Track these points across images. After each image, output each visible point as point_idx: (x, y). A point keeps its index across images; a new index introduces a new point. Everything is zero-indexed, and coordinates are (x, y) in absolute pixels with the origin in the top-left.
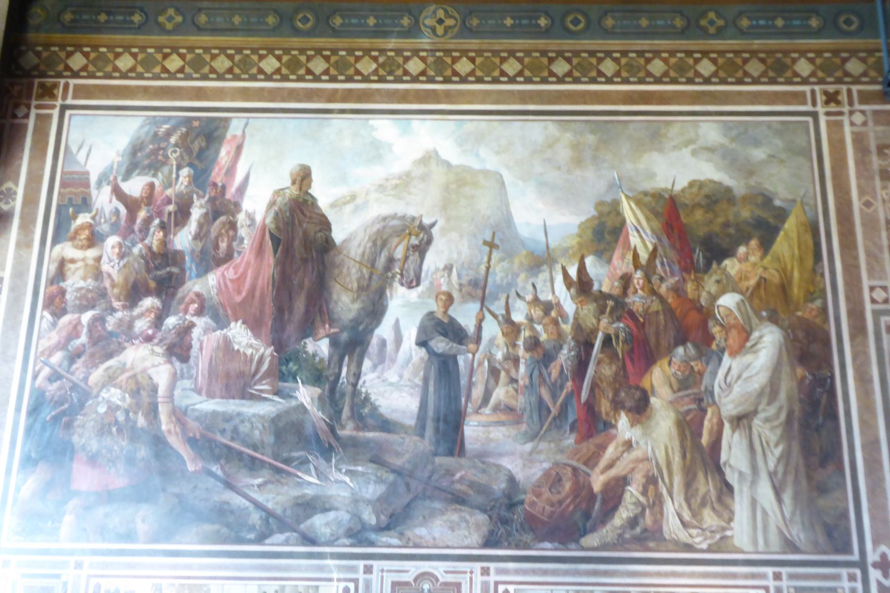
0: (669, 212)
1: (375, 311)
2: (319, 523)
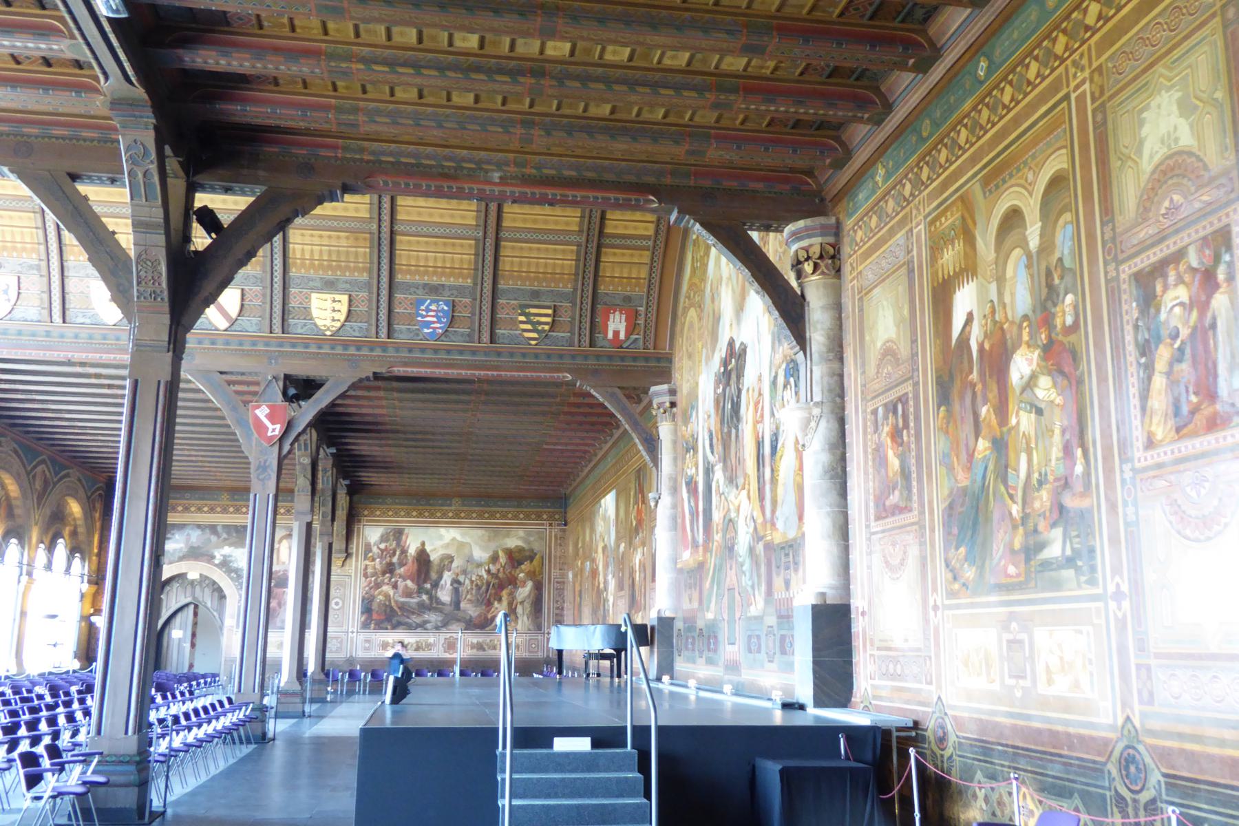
0: (510, 553)
1: (441, 577)
2: (428, 626)
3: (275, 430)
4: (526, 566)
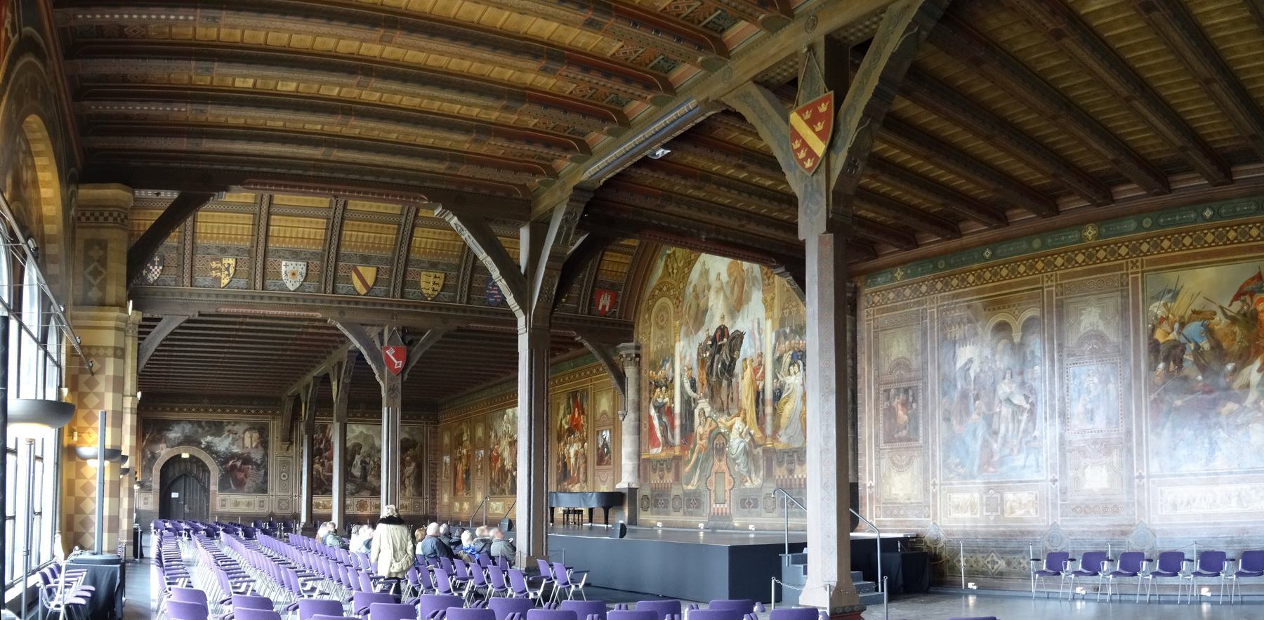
3: (399, 364)
4: (410, 452)
